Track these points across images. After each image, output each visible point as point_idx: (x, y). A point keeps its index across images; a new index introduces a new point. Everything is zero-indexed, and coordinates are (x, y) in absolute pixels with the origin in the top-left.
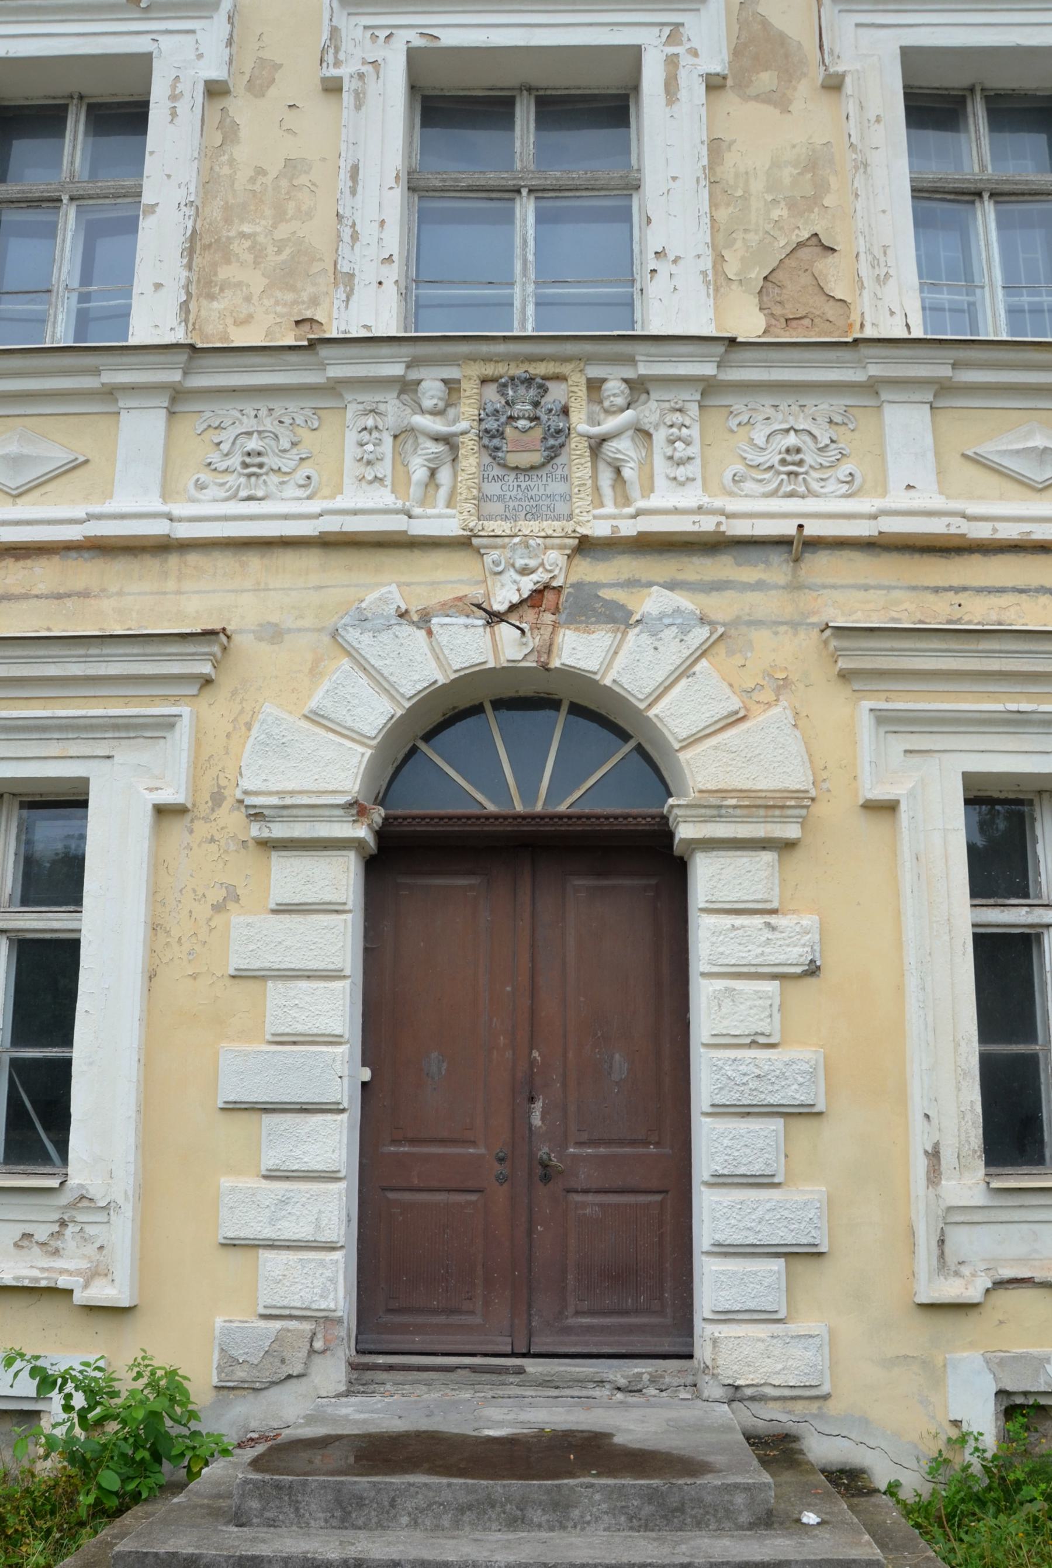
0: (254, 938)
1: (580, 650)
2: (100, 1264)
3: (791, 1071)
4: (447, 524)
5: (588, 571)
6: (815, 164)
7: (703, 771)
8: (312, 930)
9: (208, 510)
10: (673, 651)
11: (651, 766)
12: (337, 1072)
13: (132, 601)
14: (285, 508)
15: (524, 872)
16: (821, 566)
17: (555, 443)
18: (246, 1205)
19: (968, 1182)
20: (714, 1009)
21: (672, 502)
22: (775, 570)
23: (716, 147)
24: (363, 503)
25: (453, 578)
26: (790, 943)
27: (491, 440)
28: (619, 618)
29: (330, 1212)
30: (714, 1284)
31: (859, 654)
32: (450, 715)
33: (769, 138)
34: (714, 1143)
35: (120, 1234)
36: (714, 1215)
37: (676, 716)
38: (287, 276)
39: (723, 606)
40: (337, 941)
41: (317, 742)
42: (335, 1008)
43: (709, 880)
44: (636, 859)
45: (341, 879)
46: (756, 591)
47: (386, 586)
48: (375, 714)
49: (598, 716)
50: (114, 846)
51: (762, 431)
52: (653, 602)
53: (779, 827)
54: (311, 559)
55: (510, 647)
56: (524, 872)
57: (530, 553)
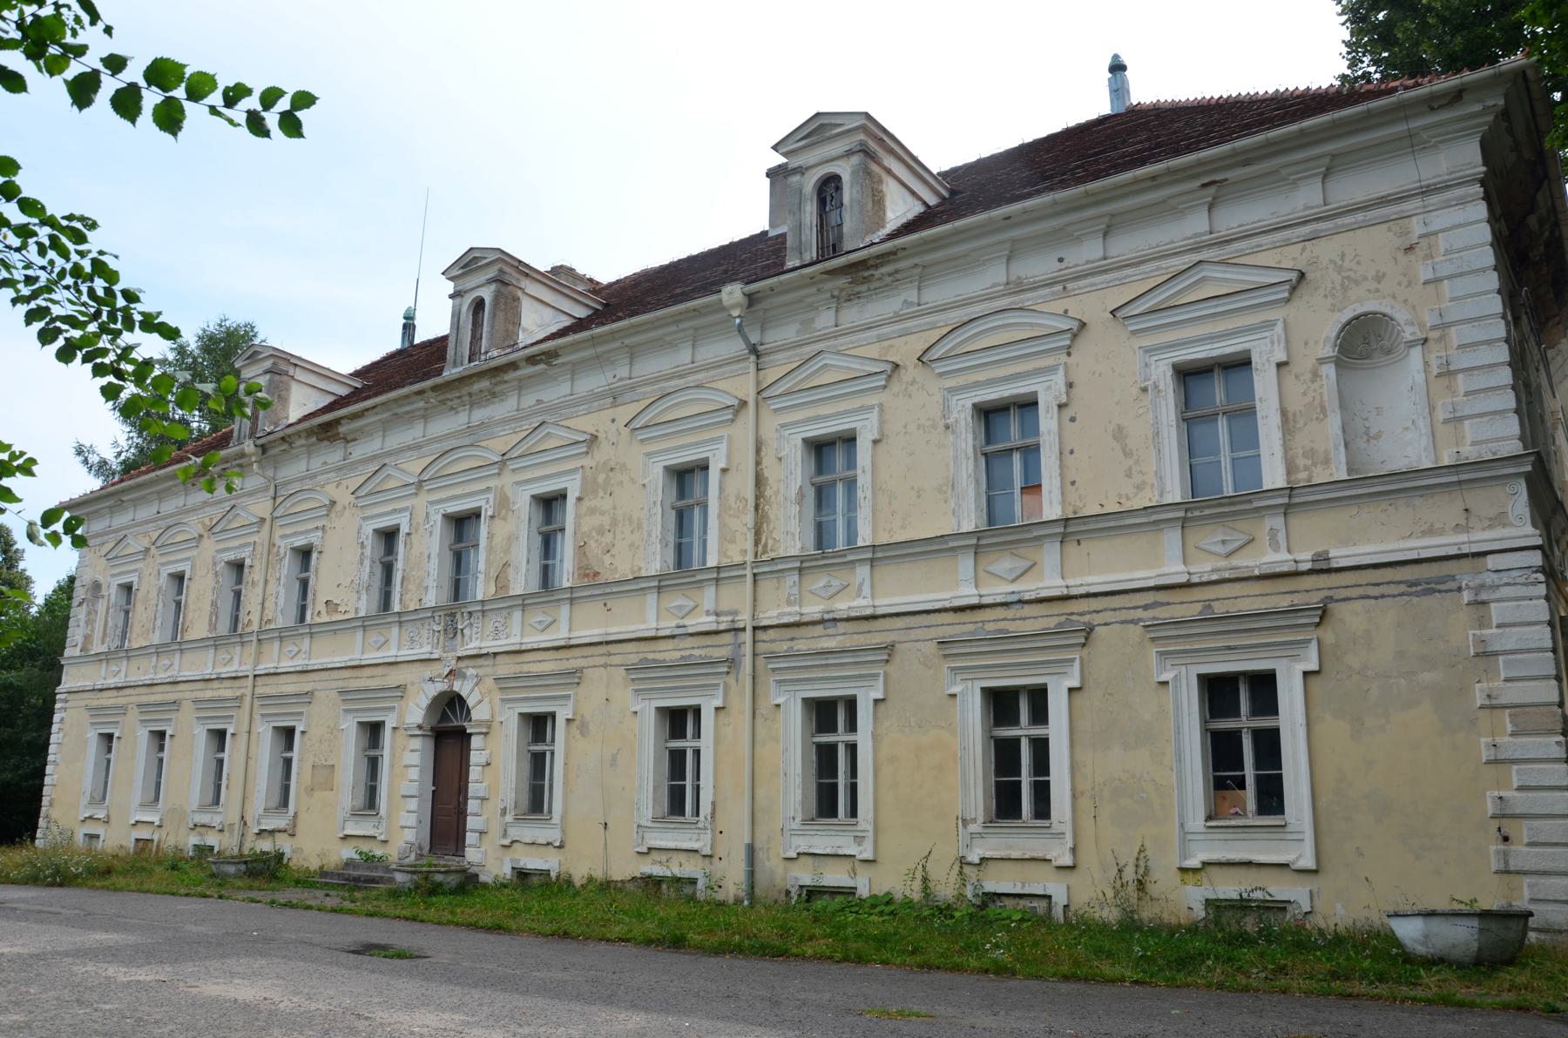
5: (462, 664)
7: (475, 715)
16: (498, 658)
20: (474, 773)
21: (472, 646)
24: (423, 651)
26: (483, 760)
28: (464, 677)
30: (470, 838)
52: (471, 672)
54: (417, 665)
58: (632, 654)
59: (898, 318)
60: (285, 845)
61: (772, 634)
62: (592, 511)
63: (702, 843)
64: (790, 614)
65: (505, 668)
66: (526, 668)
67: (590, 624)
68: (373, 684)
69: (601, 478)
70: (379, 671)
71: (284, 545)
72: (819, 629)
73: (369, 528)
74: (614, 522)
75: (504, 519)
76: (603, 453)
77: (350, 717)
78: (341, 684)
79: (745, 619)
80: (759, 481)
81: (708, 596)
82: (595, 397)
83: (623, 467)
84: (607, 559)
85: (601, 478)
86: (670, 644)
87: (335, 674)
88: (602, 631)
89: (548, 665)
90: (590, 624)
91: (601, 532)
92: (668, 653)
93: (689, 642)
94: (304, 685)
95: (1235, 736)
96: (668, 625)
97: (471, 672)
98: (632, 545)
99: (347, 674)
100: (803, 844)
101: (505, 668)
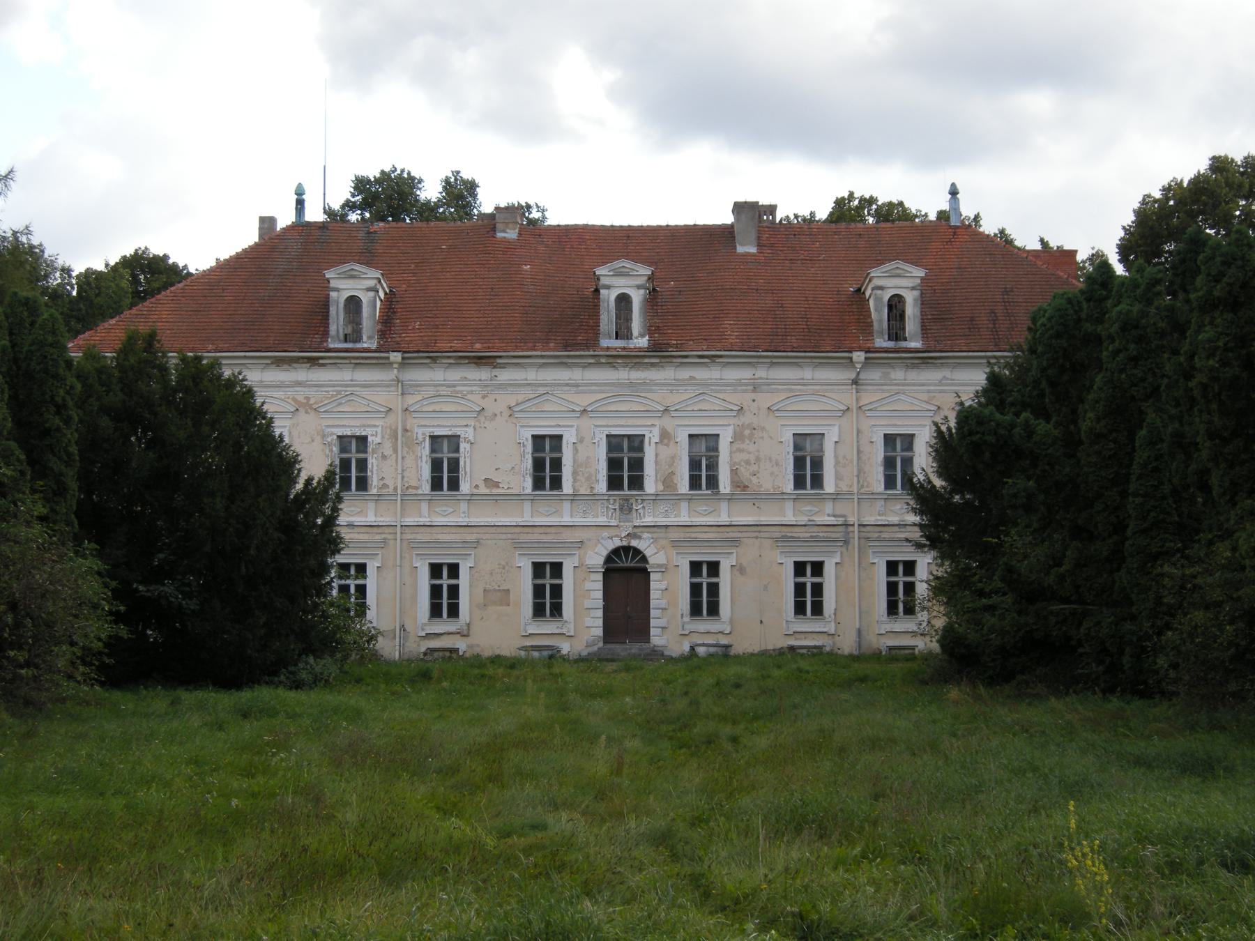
0: (588, 585)
1: (634, 543)
2: (569, 629)
3: (663, 603)
4: (614, 523)
5: (636, 530)
6: (673, 458)
7: (651, 561)
8: (595, 586)
9: (578, 520)
10: (648, 543)
11: (644, 559)
12: (601, 603)
13: (569, 536)
14: (590, 520)
15: (626, 574)
16: (670, 529)
17: (631, 510)
18: (588, 622)
19: (687, 619)
21: (648, 520)
22: (663, 530)
23: (657, 455)
24: (602, 520)
25: (614, 532)
26: (663, 585)
27: (621, 509)
28: (640, 538)
29: (600, 622)
30: (653, 632)
31: (675, 544)
32: (616, 552)
33: (665, 452)
34: (653, 613)
35: (572, 626)
36: (653, 622)
37: (648, 553)
38: (588, 478)
39: (655, 535)
40: (600, 585)
41: (596, 557)
42: (600, 595)
43: (652, 576)
44: (644, 573)
45: (600, 577)
46: (661, 533)
47: (605, 534)
48: (605, 553)
49: (637, 552)
50: (567, 571)
51: (662, 507)
52: (645, 535)
53: (663, 569)
55: (625, 543)
56: (626, 574)
57: (626, 529)
58: (777, 532)
59: (940, 383)
60: (461, 645)
61: (868, 528)
62: (741, 451)
63: (831, 628)
64: (882, 520)
65: (675, 535)
66: (693, 535)
67: (745, 515)
68: (545, 538)
69: (747, 432)
70: (553, 530)
71: (422, 432)
72: (896, 529)
73: (527, 434)
74: (758, 459)
75: (667, 445)
76: (746, 419)
77: (526, 558)
78: (515, 536)
79: (852, 519)
80: (859, 452)
81: (829, 507)
82: (739, 382)
83: (763, 429)
84: (754, 480)
85: (747, 432)
86: (803, 529)
87: (504, 530)
88: (756, 518)
89: (711, 536)
90: (745, 515)
91: (748, 462)
92: (803, 534)
93: (816, 529)
94: (470, 536)
95: (804, 584)
96: (803, 520)
97: (645, 535)
98: (772, 474)
99: (517, 530)
100: (889, 627)
101: (675, 535)
